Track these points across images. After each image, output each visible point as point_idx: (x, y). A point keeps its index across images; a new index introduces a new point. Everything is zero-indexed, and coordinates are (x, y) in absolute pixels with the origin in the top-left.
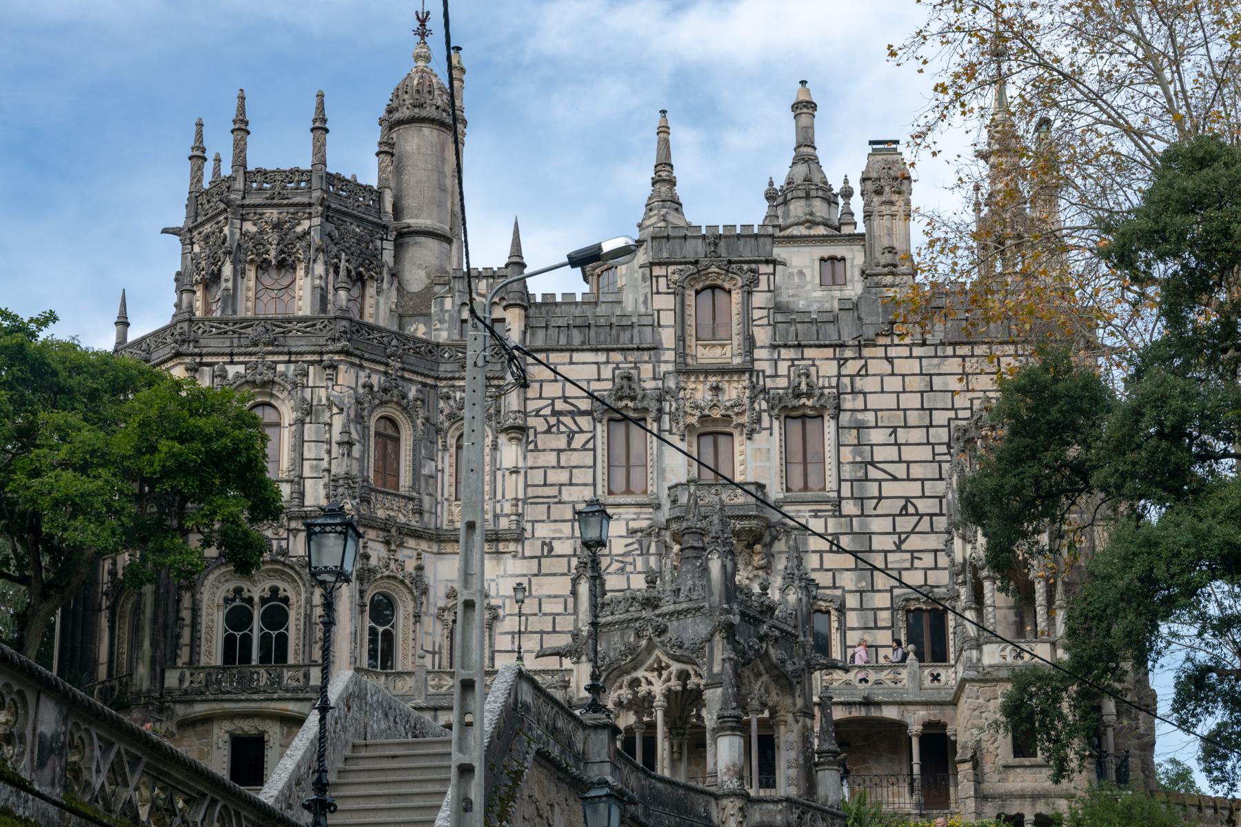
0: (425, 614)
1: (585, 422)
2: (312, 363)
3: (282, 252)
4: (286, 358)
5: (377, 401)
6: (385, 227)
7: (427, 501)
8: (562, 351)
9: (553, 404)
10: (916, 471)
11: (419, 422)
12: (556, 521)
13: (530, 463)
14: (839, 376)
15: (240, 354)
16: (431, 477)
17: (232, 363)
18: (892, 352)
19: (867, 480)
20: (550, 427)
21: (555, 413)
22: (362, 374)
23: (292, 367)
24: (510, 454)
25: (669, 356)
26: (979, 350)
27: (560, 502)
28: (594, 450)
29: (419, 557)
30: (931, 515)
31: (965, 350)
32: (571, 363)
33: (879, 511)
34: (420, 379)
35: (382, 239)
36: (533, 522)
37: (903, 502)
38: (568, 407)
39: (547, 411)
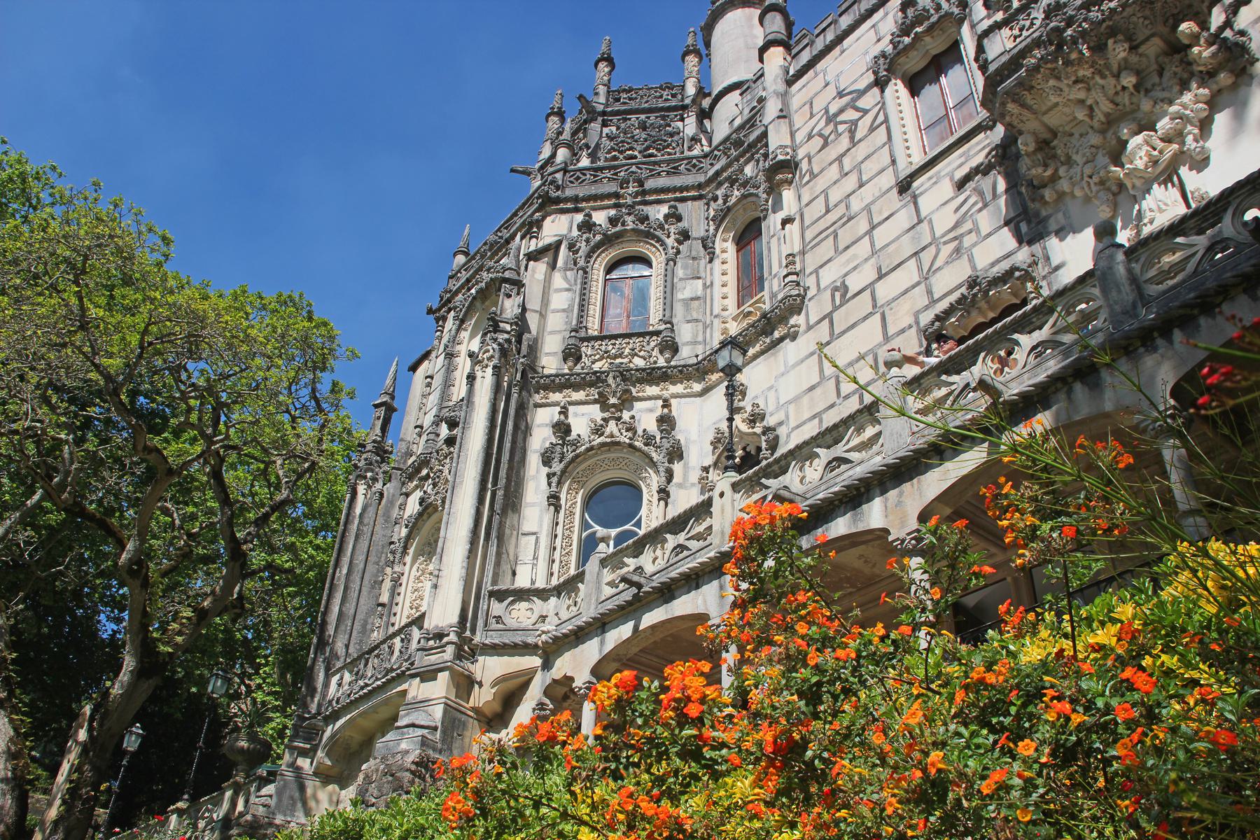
0: (680, 486)
5: (598, 237)
6: (684, 108)
7: (684, 333)
9: (827, 111)
11: (670, 242)
12: (847, 247)
13: (805, 200)
16: (697, 298)
20: (826, 139)
22: (579, 217)
27: (850, 219)
28: (886, 120)
29: (666, 404)
32: (842, 52)
34: (670, 196)
35: (682, 120)
36: (816, 271)
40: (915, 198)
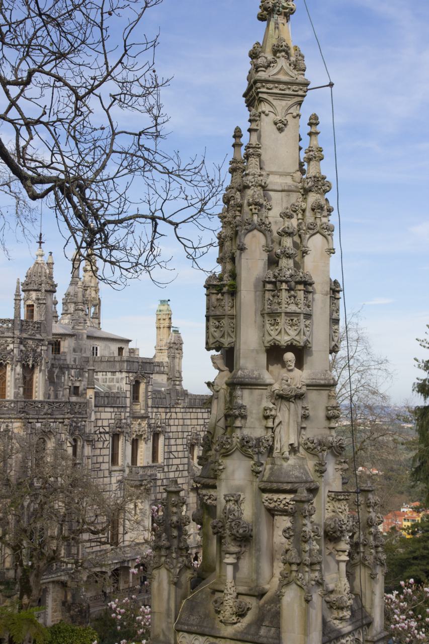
1: (107, 436)
2: (60, 422)
3: (33, 361)
4: (53, 420)
8: (102, 407)
10: (181, 455)
14: (166, 419)
15: (41, 418)
17: (38, 422)
18: (178, 410)
19: (170, 458)
21: (100, 433)
23: (55, 424)
24: (88, 450)
25: (128, 410)
26: (194, 410)
30: (182, 471)
31: (191, 410)
33: (172, 470)
37: (176, 466)
38: (103, 431)
39: (98, 432)
40: (111, 477)
